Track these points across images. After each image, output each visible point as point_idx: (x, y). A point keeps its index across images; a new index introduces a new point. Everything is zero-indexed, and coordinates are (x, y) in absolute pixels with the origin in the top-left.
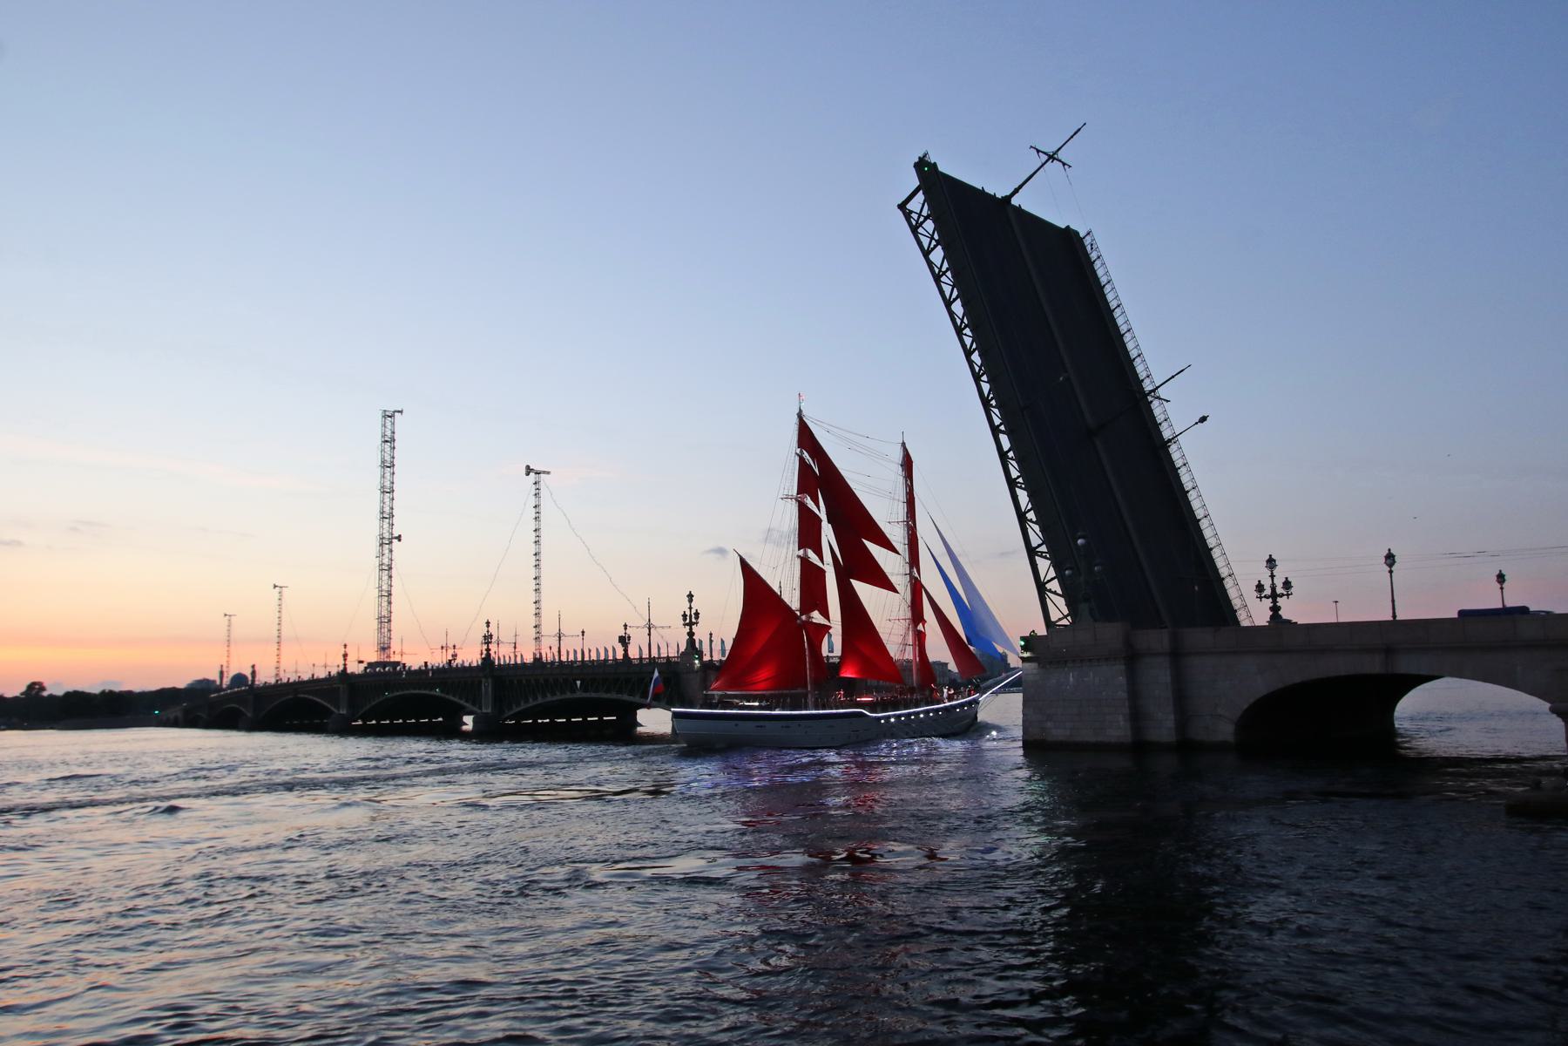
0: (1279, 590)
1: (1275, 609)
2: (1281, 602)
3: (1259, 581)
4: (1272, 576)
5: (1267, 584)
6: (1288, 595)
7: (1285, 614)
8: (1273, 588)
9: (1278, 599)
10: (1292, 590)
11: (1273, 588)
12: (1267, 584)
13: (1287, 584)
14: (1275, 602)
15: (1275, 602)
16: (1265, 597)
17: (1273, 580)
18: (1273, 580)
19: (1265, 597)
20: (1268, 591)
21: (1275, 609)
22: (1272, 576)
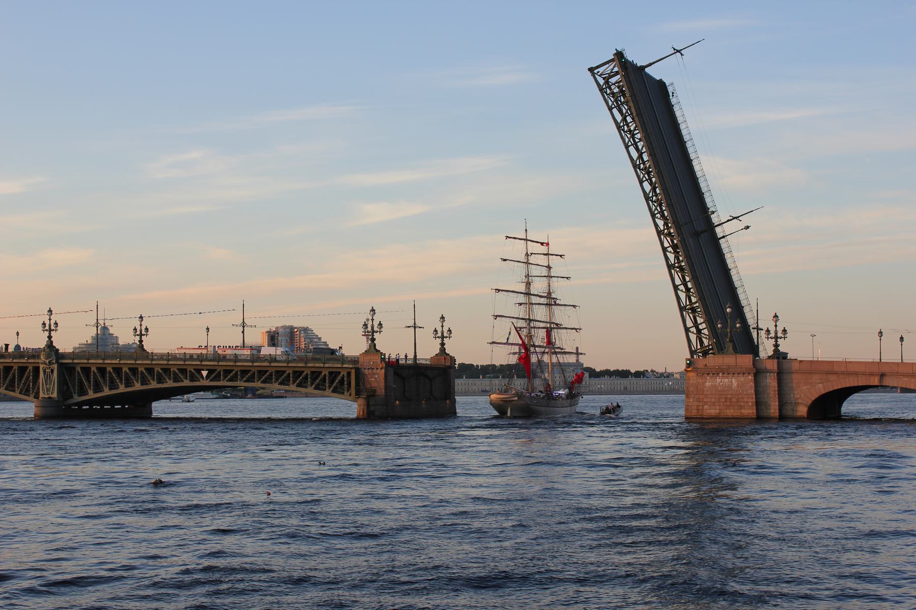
0: (779, 335)
1: (776, 346)
2: (780, 341)
3: (784, 328)
4: (776, 326)
5: (772, 329)
6: (785, 338)
7: (782, 349)
8: (776, 333)
9: (779, 340)
10: (787, 335)
11: (776, 333)
12: (772, 329)
13: (785, 331)
14: (776, 341)
15: (776, 341)
16: (771, 338)
17: (776, 328)
18: (776, 328)
19: (771, 338)
20: (773, 335)
21: (776, 346)
22: (776, 326)
